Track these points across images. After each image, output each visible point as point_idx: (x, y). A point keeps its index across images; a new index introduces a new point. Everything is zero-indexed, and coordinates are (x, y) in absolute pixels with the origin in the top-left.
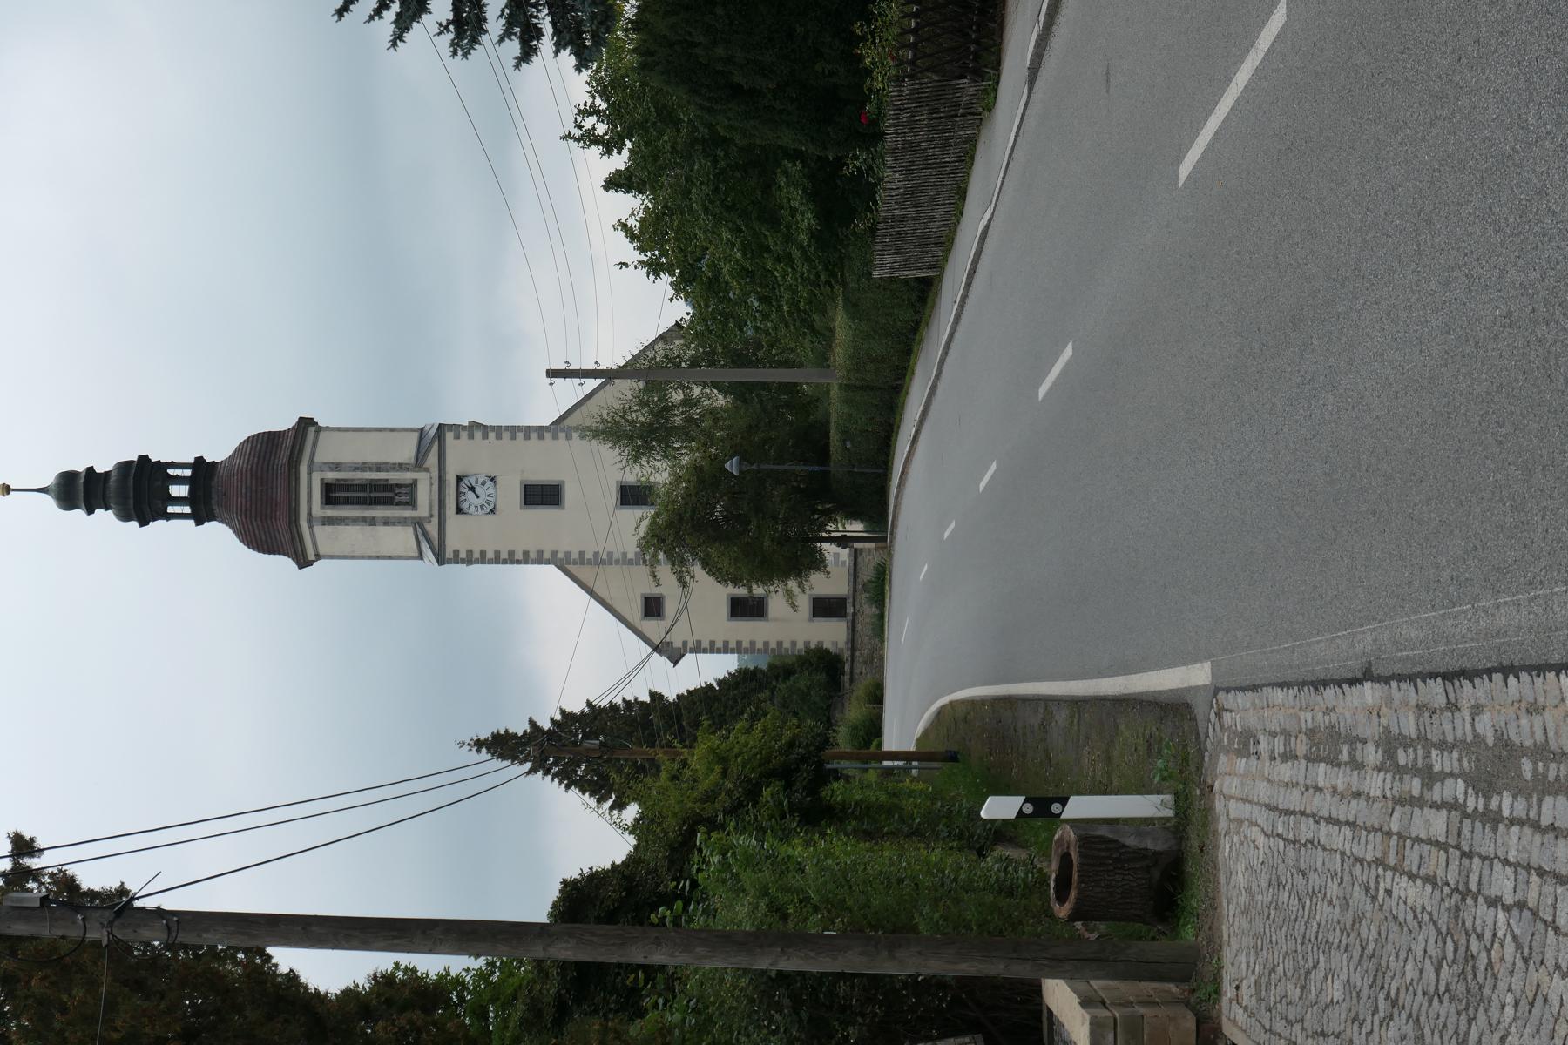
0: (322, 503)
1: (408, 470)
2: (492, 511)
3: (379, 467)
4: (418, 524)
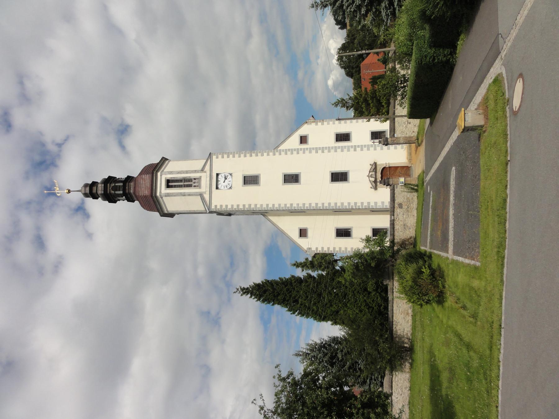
0: (165, 187)
1: (198, 172)
2: (230, 188)
3: (187, 172)
4: (201, 195)
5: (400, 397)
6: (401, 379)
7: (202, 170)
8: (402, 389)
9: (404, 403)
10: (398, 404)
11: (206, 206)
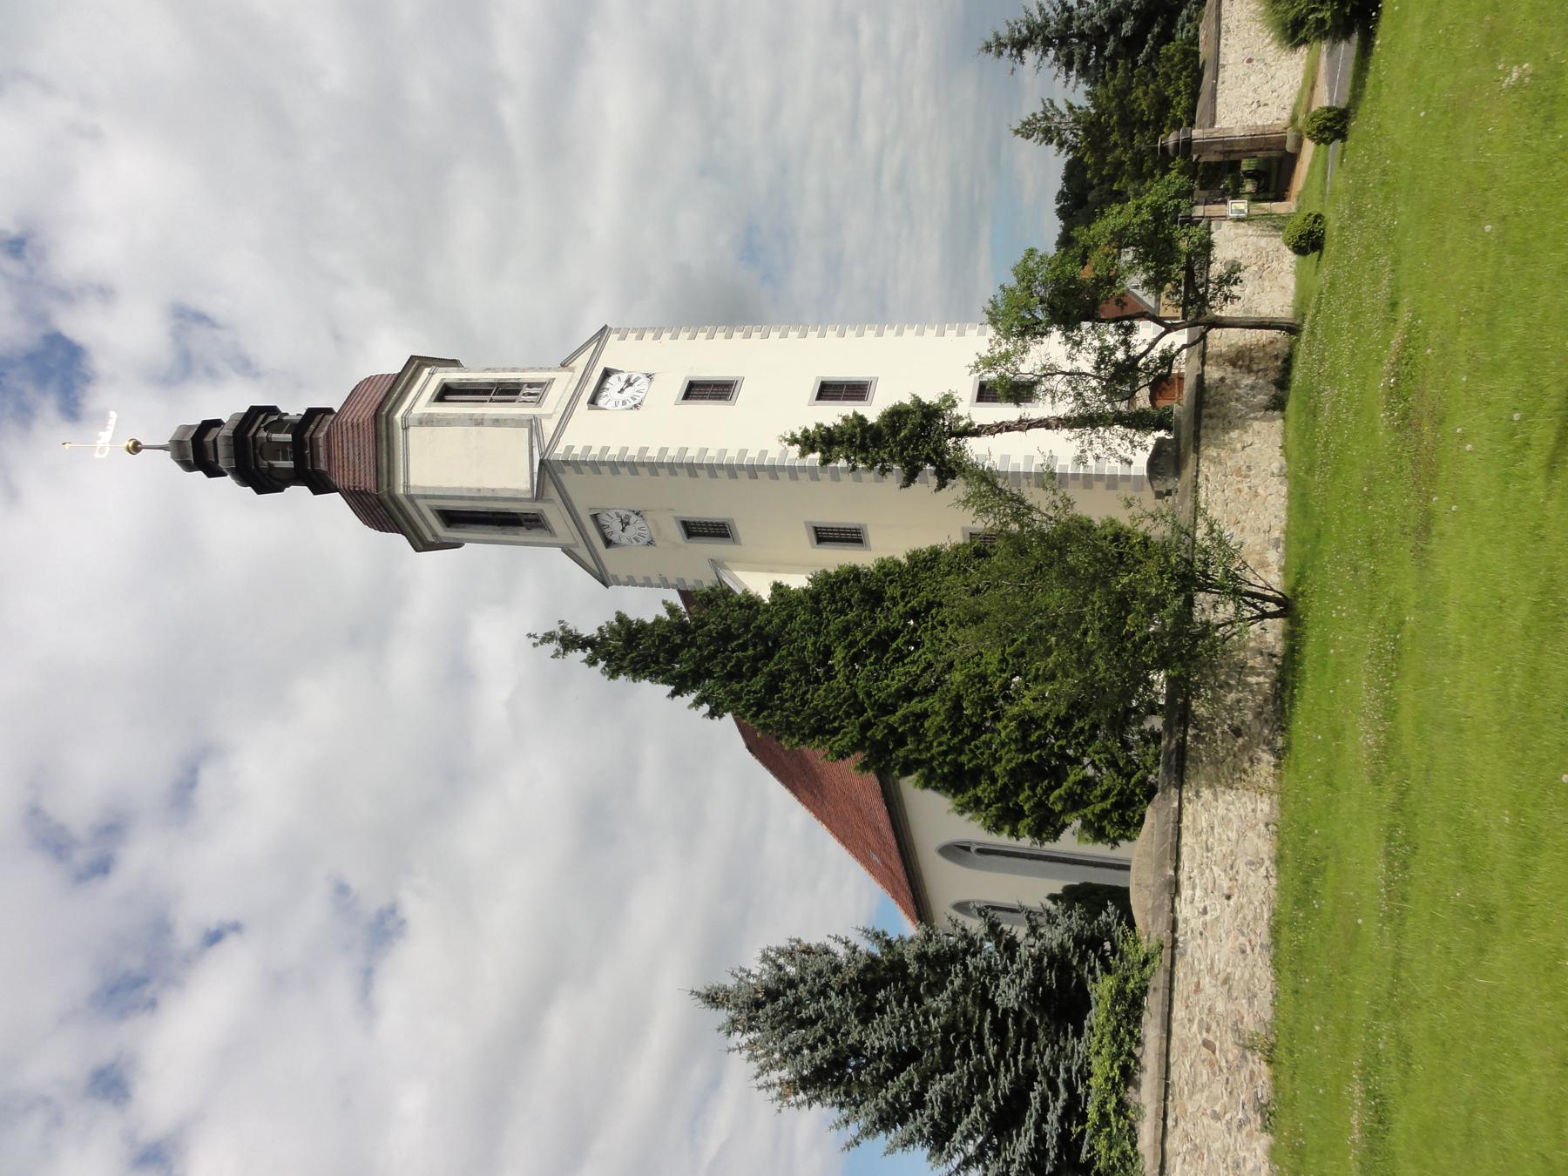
5: (1222, 910)
6: (1230, 820)
8: (1232, 868)
9: (1242, 939)
10: (1210, 941)
11: (535, 444)
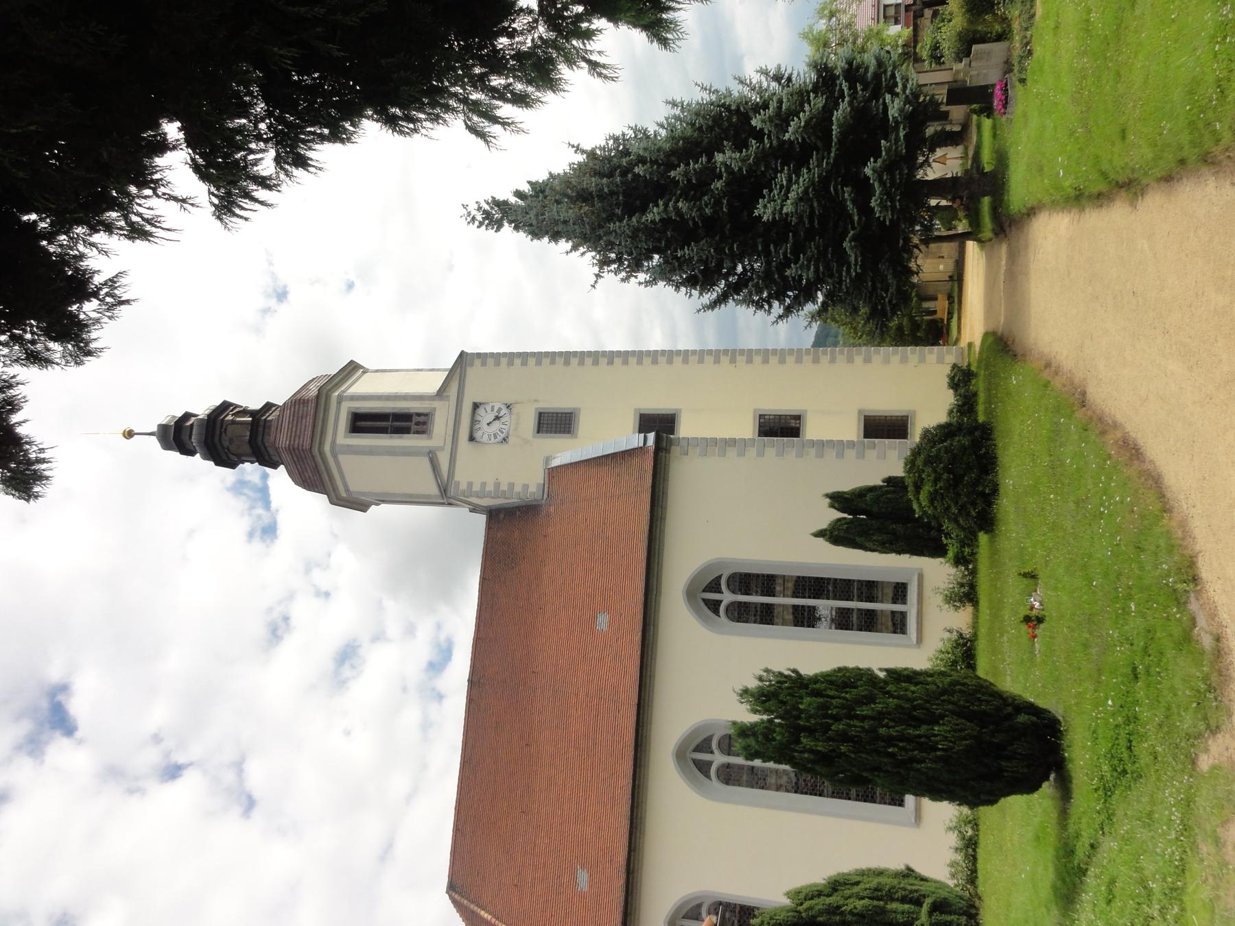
0: (345, 432)
3: (405, 397)
7: (441, 393)
